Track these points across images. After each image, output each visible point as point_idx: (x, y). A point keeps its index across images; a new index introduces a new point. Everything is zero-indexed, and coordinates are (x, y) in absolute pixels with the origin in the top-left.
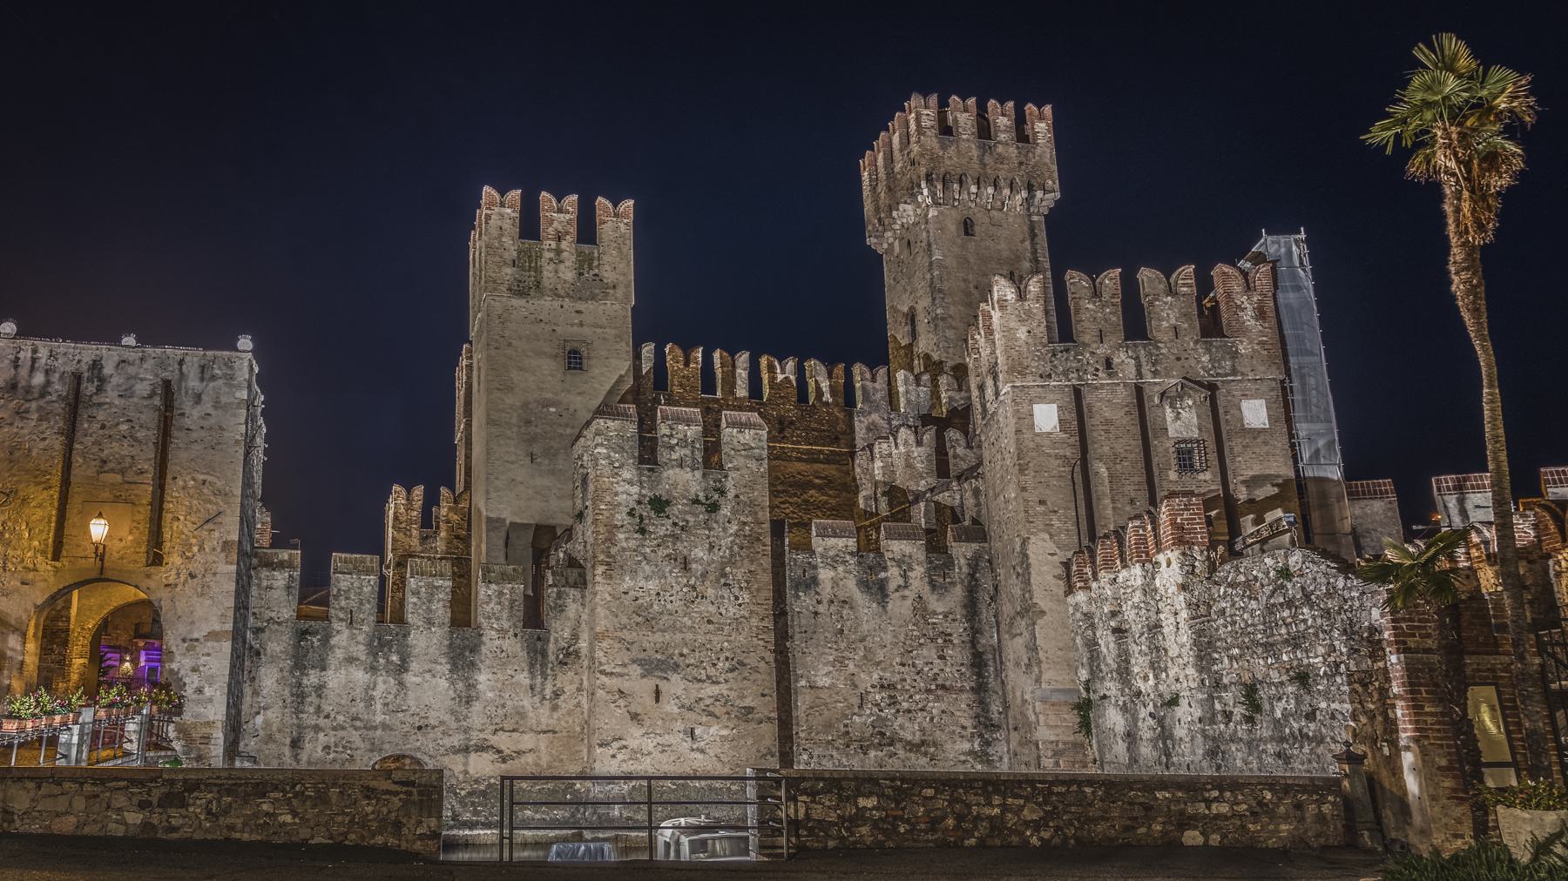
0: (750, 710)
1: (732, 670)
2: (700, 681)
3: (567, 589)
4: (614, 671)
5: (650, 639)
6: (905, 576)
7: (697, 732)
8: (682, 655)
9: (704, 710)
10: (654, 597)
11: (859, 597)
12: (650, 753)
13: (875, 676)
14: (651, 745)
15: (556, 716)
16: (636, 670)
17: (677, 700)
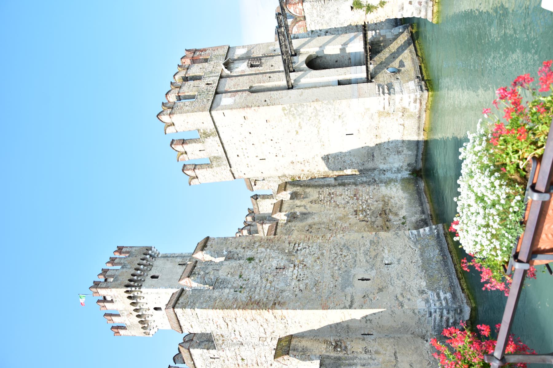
0: (372, 242)
1: (348, 249)
2: (355, 261)
3: (292, 345)
4: (349, 300)
5: (327, 284)
6: (299, 206)
7: (387, 263)
8: (339, 269)
9: (374, 259)
10: (300, 281)
11: (310, 221)
12: (404, 282)
13: (351, 216)
14: (398, 282)
15: (382, 351)
16: (349, 290)
17: (368, 271)
